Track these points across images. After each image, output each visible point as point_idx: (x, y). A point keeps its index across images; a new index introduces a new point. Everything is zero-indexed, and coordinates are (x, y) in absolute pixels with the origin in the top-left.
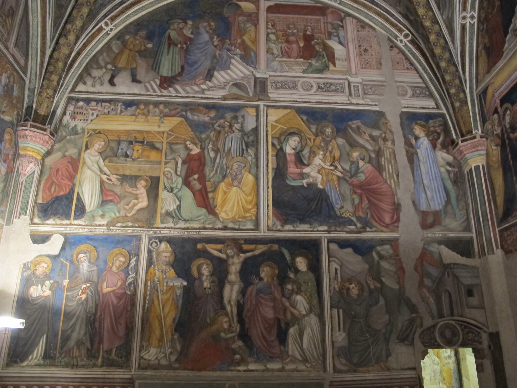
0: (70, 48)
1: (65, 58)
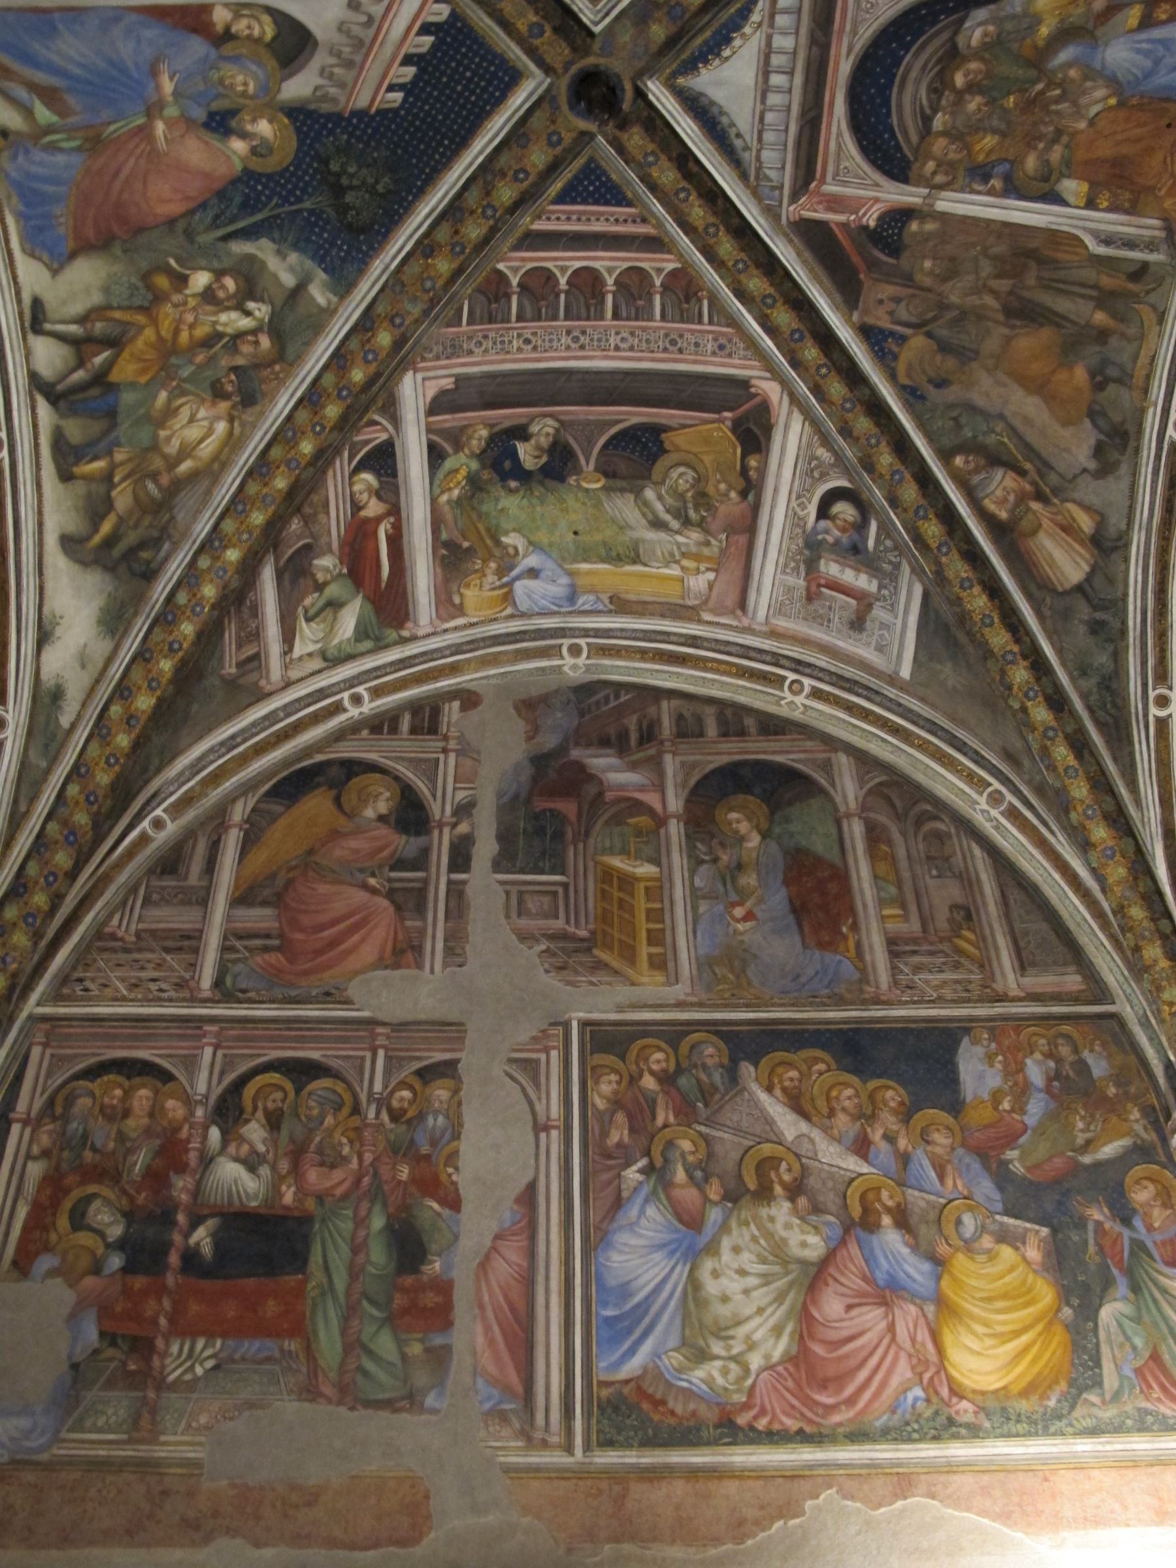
0: (1118, 857)
1: (1131, 888)
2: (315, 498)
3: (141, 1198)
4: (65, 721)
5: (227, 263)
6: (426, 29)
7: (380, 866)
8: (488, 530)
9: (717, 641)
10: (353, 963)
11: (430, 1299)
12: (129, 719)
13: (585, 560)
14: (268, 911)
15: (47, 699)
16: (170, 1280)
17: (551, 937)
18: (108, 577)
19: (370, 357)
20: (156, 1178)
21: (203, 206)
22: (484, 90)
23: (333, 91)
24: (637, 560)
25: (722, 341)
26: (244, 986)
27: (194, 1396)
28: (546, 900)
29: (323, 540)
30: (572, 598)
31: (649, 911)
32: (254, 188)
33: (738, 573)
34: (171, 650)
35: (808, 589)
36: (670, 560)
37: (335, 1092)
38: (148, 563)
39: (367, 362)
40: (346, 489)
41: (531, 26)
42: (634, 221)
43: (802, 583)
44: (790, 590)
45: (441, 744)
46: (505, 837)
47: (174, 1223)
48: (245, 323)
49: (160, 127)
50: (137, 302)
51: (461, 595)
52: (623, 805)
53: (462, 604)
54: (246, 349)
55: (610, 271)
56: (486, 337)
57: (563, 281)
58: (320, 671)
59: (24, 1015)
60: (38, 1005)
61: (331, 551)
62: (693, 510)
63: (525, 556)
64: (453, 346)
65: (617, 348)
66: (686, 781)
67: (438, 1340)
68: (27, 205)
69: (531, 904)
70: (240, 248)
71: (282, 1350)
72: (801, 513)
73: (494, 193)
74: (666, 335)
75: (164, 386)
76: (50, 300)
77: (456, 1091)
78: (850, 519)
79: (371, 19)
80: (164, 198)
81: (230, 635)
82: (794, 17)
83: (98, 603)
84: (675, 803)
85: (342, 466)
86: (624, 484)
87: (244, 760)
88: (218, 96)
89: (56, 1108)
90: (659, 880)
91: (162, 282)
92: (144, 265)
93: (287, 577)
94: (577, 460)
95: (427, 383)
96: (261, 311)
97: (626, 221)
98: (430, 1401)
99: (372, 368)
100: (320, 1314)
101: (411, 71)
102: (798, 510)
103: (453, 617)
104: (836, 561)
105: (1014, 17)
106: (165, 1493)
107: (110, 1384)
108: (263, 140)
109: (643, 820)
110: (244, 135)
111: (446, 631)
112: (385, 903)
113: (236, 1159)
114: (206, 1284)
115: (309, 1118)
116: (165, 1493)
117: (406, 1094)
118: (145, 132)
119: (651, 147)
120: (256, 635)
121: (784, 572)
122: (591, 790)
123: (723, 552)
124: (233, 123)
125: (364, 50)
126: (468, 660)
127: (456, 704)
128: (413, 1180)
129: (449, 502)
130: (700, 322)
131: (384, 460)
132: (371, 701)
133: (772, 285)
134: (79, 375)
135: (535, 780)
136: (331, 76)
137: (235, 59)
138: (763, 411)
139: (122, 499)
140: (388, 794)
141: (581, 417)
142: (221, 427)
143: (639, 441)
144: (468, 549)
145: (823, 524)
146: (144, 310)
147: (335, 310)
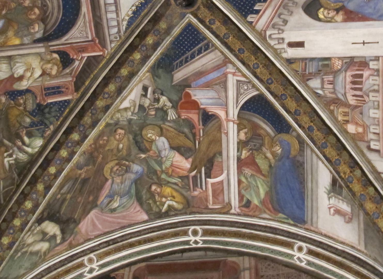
6: (257, 12)
41: (214, 23)
79: (279, 16)
82: (109, 25)
105: (25, 36)
125: (283, 4)
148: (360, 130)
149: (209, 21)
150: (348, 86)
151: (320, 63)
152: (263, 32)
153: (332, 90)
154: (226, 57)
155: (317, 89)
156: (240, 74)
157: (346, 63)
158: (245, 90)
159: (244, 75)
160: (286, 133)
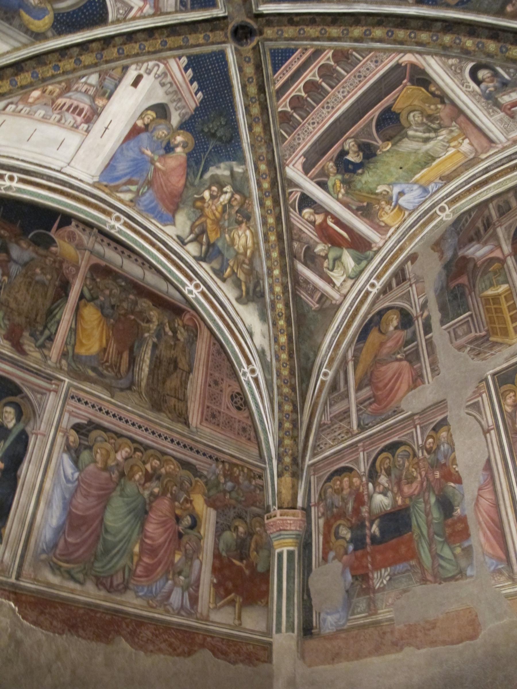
2: (295, 231)
3: (354, 520)
4: (269, 359)
5: (208, 184)
7: (400, 348)
8: (368, 193)
9: (496, 163)
10: (400, 394)
11: (460, 526)
12: (282, 348)
13: (415, 174)
14: (368, 388)
15: (262, 354)
16: (369, 549)
17: (470, 343)
18: (254, 304)
19: (264, 176)
20: (357, 511)
21: (188, 174)
22: (219, 66)
23: (184, 111)
24: (434, 159)
25: (374, 59)
26: (366, 422)
27: (385, 593)
28: (465, 327)
29: (311, 242)
30: (425, 190)
31: (509, 307)
32: (193, 157)
33: (475, 131)
34: (279, 316)
35: (507, 114)
36: (446, 149)
37: (405, 451)
38: (260, 291)
39: (265, 179)
40: (303, 221)
41: (204, 38)
42: (303, 53)
43: (502, 114)
44: (501, 120)
45: (409, 283)
46: (442, 309)
47: (365, 526)
48: (228, 196)
49: (158, 164)
50: (198, 215)
51: (383, 221)
52: (486, 264)
53: (386, 224)
54: (235, 203)
55: (314, 75)
56: (299, 135)
57: (303, 94)
58: (354, 284)
59: (306, 466)
60: (309, 460)
61: (317, 243)
62: (432, 124)
63: (392, 191)
64: (292, 147)
65: (344, 97)
66: (509, 235)
67: (466, 544)
68: (153, 213)
69: (460, 332)
70: (207, 176)
71: (411, 566)
72: (471, 89)
73: (249, 94)
74: (355, 76)
75: (225, 233)
76: (179, 233)
77: (449, 430)
78: (489, 75)
80: (177, 181)
81: (304, 295)
83: (256, 313)
84: (507, 248)
85: (294, 215)
86: (398, 138)
87: (344, 333)
88: (161, 143)
89: (322, 497)
90: (510, 289)
91: (199, 204)
92: (190, 203)
93: (309, 263)
94: (372, 144)
95: (296, 165)
96: (228, 189)
97: (301, 56)
98: (469, 572)
99: (268, 179)
100: (420, 545)
101: (195, 84)
102: (468, 89)
103: (388, 231)
104: (504, 95)
106: (384, 633)
107: (359, 595)
108: (183, 142)
109: (496, 265)
110: (177, 146)
111: (390, 237)
112: (405, 363)
113: (380, 493)
114: (381, 546)
115: (399, 466)
116: (384, 633)
117: (431, 440)
118: (156, 169)
119: (276, 29)
120: (316, 288)
121: (491, 116)
122: (471, 265)
123: (460, 128)
124: (172, 145)
126: (405, 243)
127: (409, 263)
128: (442, 477)
129: (343, 195)
130: (360, 61)
131: (306, 201)
132: (378, 282)
133: (362, 26)
134: (204, 248)
135: (447, 276)
136: (179, 108)
137: (154, 129)
138: (414, 66)
139: (242, 276)
140: (395, 317)
141: (358, 129)
142: (248, 232)
143: (387, 119)
144: (368, 204)
145: (483, 86)
146: (201, 216)
147: (247, 170)
148: (31, 100)
149: (209, 36)
150: (75, 103)
151: (109, 91)
152: (165, 62)
153: (79, 89)
154: (162, 14)
155: (88, 78)
156: (138, 15)
157: (98, 109)
158: (118, 9)
159: (134, 18)
160: (53, 24)
